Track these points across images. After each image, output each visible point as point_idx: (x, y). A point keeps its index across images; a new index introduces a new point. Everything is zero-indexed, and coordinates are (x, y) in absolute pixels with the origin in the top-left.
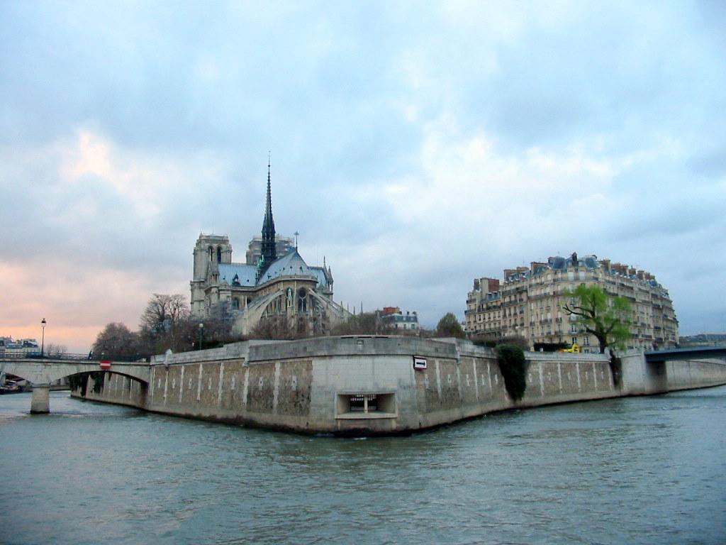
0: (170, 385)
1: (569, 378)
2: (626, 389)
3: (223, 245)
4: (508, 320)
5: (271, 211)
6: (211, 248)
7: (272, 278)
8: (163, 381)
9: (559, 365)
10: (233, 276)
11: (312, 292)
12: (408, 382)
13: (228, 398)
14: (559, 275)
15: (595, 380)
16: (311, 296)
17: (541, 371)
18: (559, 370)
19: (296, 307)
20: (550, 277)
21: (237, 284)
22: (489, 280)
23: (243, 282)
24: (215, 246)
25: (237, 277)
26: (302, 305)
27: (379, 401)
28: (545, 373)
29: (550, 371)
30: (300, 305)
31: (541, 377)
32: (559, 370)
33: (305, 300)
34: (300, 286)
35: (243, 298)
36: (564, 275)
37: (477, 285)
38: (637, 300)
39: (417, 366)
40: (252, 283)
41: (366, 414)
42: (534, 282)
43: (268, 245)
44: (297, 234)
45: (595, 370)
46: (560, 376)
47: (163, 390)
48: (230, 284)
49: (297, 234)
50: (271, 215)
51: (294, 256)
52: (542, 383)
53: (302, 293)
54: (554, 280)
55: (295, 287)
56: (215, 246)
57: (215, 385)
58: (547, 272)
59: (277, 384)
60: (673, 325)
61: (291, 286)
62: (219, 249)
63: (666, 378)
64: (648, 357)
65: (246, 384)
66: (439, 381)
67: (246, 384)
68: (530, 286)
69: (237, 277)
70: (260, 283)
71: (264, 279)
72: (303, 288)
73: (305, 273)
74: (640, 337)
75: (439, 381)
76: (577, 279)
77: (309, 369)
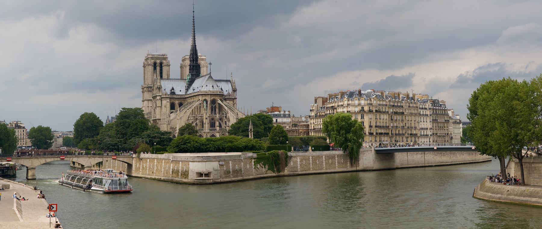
0: (143, 167)
5: (195, 43)
6: (155, 64)
7: (195, 91)
9: (311, 157)
10: (171, 88)
11: (220, 102)
12: (216, 169)
13: (165, 172)
14: (350, 102)
15: (337, 163)
16: (219, 104)
17: (299, 160)
18: (311, 160)
19: (209, 111)
20: (346, 103)
21: (173, 93)
23: (177, 92)
24: (158, 61)
25: (173, 89)
26: (213, 110)
27: (207, 175)
30: (212, 110)
31: (299, 163)
32: (311, 160)
33: (215, 106)
34: (212, 98)
35: (177, 102)
36: (353, 102)
38: (405, 113)
40: (183, 93)
42: (340, 104)
43: (193, 67)
44: (210, 64)
45: (336, 159)
46: (311, 162)
47: (139, 168)
48: (169, 93)
49: (210, 64)
50: (195, 46)
51: (209, 78)
52: (299, 166)
53: (213, 102)
54: (348, 104)
55: (209, 99)
56: (158, 61)
57: (161, 167)
58: (345, 99)
59: (180, 168)
61: (207, 98)
62: (161, 64)
63: (394, 162)
64: (378, 152)
65: (171, 168)
66: (231, 167)
67: (171, 168)
68: (338, 106)
69: (173, 89)
70: (188, 93)
71: (190, 91)
73: (215, 90)
75: (231, 167)
76: (359, 105)
77: (189, 165)
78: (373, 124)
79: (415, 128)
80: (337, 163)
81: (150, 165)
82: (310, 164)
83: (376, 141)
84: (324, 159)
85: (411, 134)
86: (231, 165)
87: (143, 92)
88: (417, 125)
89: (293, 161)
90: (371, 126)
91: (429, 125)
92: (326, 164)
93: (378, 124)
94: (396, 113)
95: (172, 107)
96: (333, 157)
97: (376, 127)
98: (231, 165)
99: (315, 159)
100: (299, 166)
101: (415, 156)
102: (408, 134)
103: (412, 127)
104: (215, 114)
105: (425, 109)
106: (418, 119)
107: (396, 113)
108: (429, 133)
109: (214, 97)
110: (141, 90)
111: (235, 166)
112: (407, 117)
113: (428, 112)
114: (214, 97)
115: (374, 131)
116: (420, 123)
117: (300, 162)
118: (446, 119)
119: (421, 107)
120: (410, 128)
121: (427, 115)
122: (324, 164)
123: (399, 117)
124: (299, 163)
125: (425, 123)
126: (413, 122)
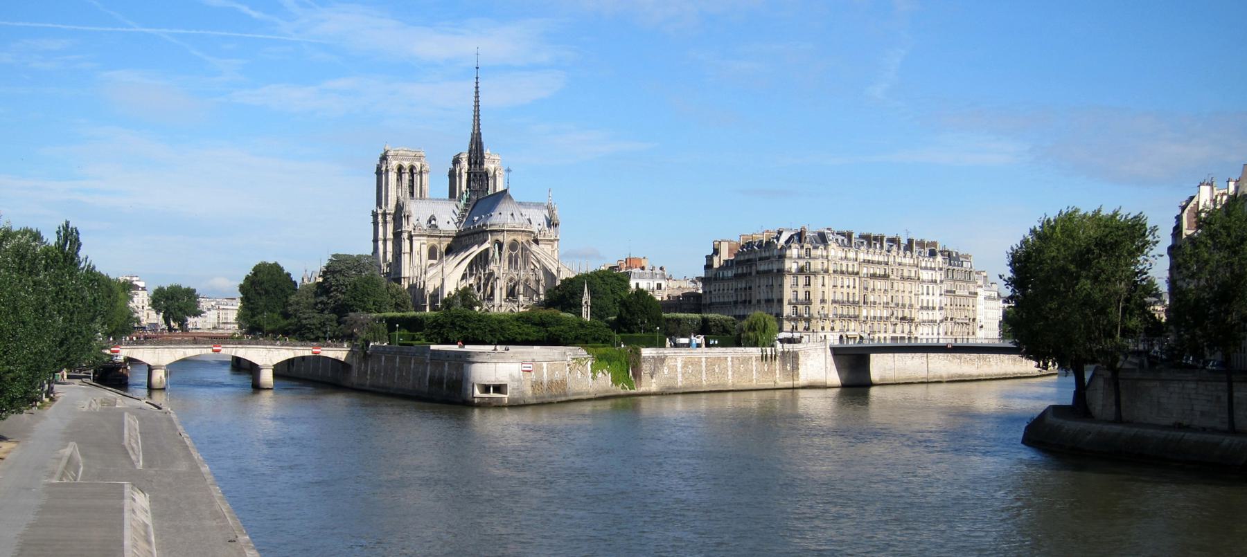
0: (372, 370)
2: (803, 379)
6: (400, 169)
8: (366, 366)
17: (679, 365)
24: (406, 164)
25: (433, 218)
27: (499, 388)
28: (685, 366)
30: (510, 262)
31: (679, 370)
32: (704, 364)
33: (517, 255)
34: (512, 238)
41: (492, 395)
44: (508, 170)
52: (680, 375)
56: (406, 164)
64: (835, 351)
66: (545, 375)
75: (545, 375)
78: (829, 297)
79: (911, 306)
82: (701, 372)
83: (833, 329)
85: (903, 319)
86: (545, 370)
91: (936, 299)
92: (734, 373)
93: (839, 297)
94: (874, 276)
95: (432, 253)
96: (746, 360)
97: (834, 302)
98: (545, 370)
99: (711, 363)
100: (680, 375)
103: (904, 306)
105: (932, 269)
106: (915, 287)
107: (874, 276)
109: (515, 237)
111: (553, 372)
112: (895, 285)
113: (938, 276)
114: (515, 237)
115: (830, 309)
116: (921, 297)
118: (972, 290)
119: (923, 265)
123: (879, 284)
125: (930, 298)
126: (906, 293)
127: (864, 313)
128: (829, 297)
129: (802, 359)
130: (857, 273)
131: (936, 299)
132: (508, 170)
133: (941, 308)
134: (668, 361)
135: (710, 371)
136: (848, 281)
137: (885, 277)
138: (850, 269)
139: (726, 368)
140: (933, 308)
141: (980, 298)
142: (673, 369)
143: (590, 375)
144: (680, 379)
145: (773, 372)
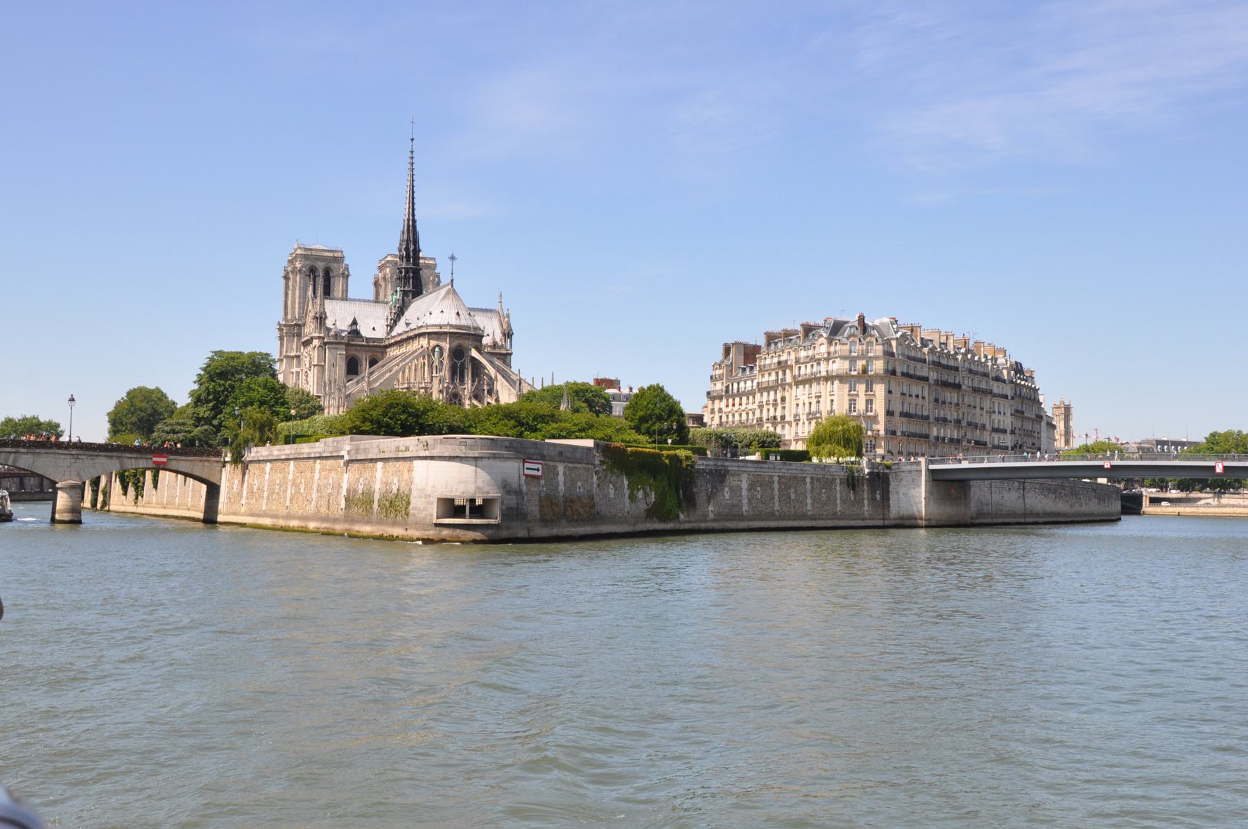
1: (793, 496)
3: (334, 265)
4: (765, 410)
5: (413, 215)
6: (313, 270)
7: (412, 326)
9: (776, 479)
10: (350, 321)
12: (515, 485)
13: (324, 502)
15: (838, 501)
16: (473, 359)
17: (745, 485)
18: (776, 486)
19: (446, 373)
20: (823, 349)
21: (355, 333)
22: (746, 346)
23: (365, 332)
24: (320, 265)
25: (355, 323)
26: (457, 372)
28: (752, 487)
29: (761, 486)
31: (744, 493)
32: (776, 486)
34: (456, 343)
37: (727, 350)
39: (527, 472)
40: (380, 333)
43: (407, 272)
44: (453, 258)
45: (838, 488)
46: (776, 492)
50: (414, 221)
51: (448, 293)
52: (745, 501)
56: (320, 265)
57: (308, 486)
58: (822, 340)
60: (1036, 427)
61: (442, 344)
66: (561, 487)
67: (345, 486)
69: (355, 323)
70: (394, 334)
71: (400, 328)
72: (459, 346)
73: (463, 322)
74: (964, 443)
75: (561, 487)
77: (410, 471)
78: (897, 408)
80: (838, 501)
81: (272, 481)
82: (773, 499)
84: (809, 486)
85: (977, 443)
86: (561, 478)
87: (281, 338)
88: (985, 420)
89: (731, 489)
90: (889, 413)
91: (1006, 421)
92: (814, 500)
94: (945, 384)
98: (561, 478)
101: (1006, 495)
102: (969, 442)
104: (462, 381)
106: (987, 404)
107: (945, 384)
108: (1008, 440)
110: (278, 334)
111: (573, 483)
116: (993, 416)
117: (749, 490)
120: (973, 425)
121: (1006, 397)
122: (809, 501)
123: (951, 396)
124: (744, 493)
125: (1001, 417)
127: (934, 432)
128: (897, 408)
129: (893, 484)
130: (926, 379)
131: (1006, 421)
132: (453, 258)
133: (1013, 432)
134: (732, 481)
135: (784, 497)
136: (916, 389)
137: (957, 387)
138: (918, 373)
139: (804, 494)
140: (1004, 431)
141: (1044, 424)
142: (736, 491)
143: (627, 492)
144: (745, 508)
145: (859, 502)
